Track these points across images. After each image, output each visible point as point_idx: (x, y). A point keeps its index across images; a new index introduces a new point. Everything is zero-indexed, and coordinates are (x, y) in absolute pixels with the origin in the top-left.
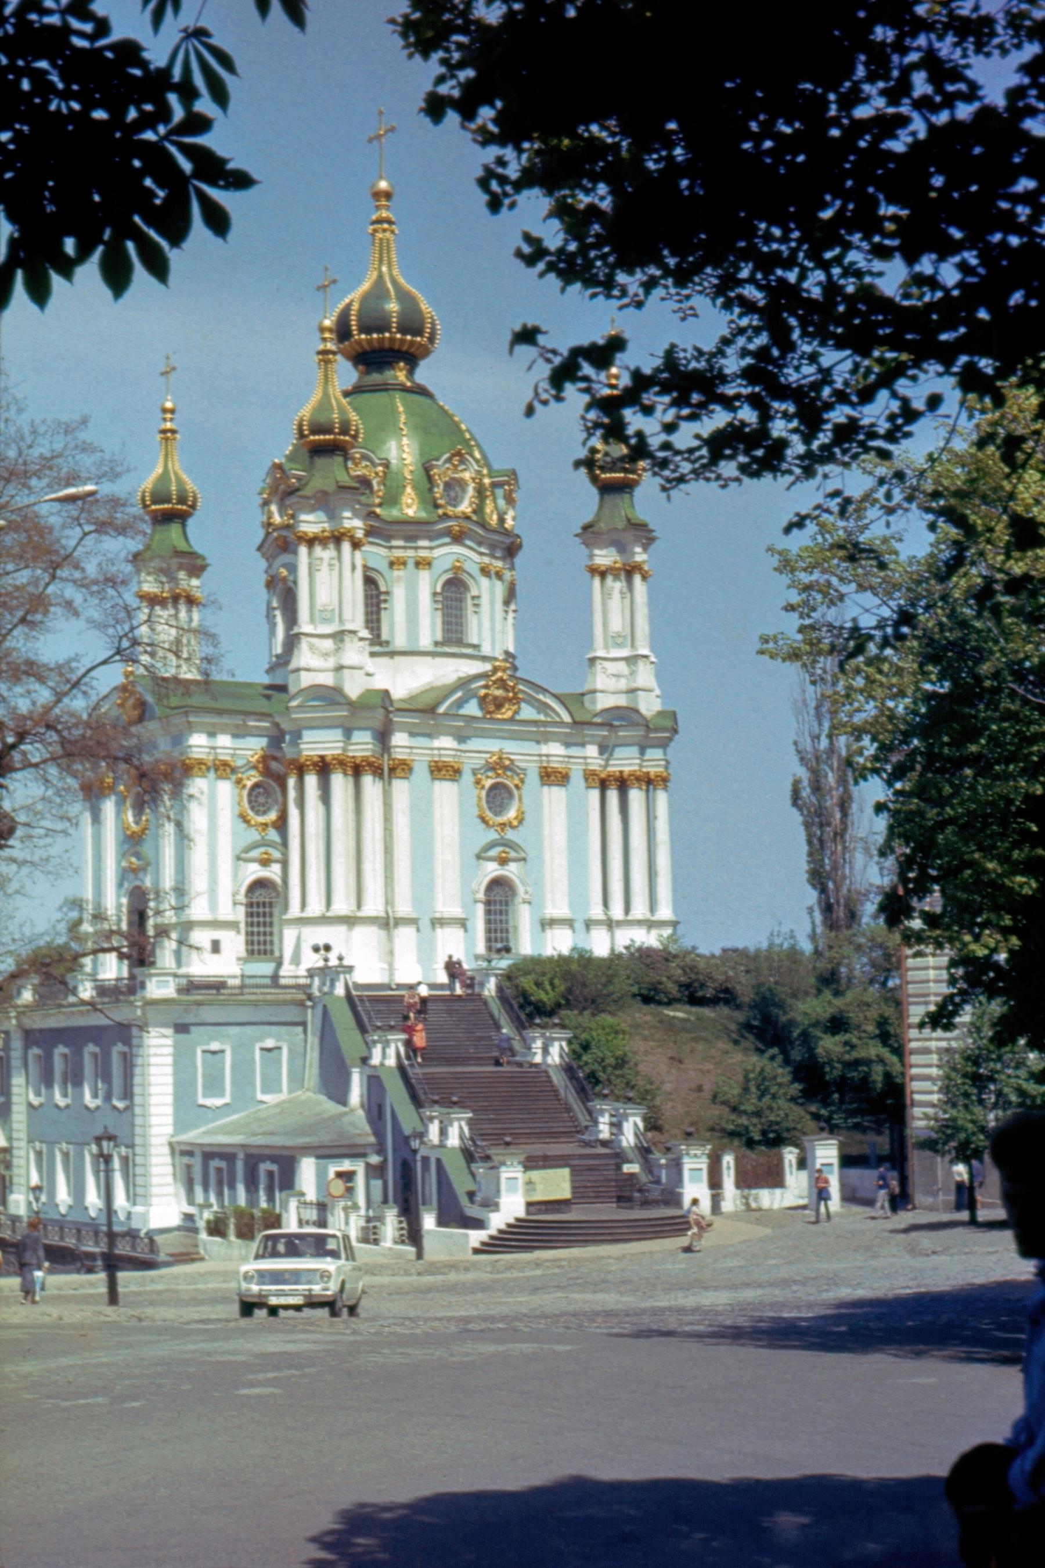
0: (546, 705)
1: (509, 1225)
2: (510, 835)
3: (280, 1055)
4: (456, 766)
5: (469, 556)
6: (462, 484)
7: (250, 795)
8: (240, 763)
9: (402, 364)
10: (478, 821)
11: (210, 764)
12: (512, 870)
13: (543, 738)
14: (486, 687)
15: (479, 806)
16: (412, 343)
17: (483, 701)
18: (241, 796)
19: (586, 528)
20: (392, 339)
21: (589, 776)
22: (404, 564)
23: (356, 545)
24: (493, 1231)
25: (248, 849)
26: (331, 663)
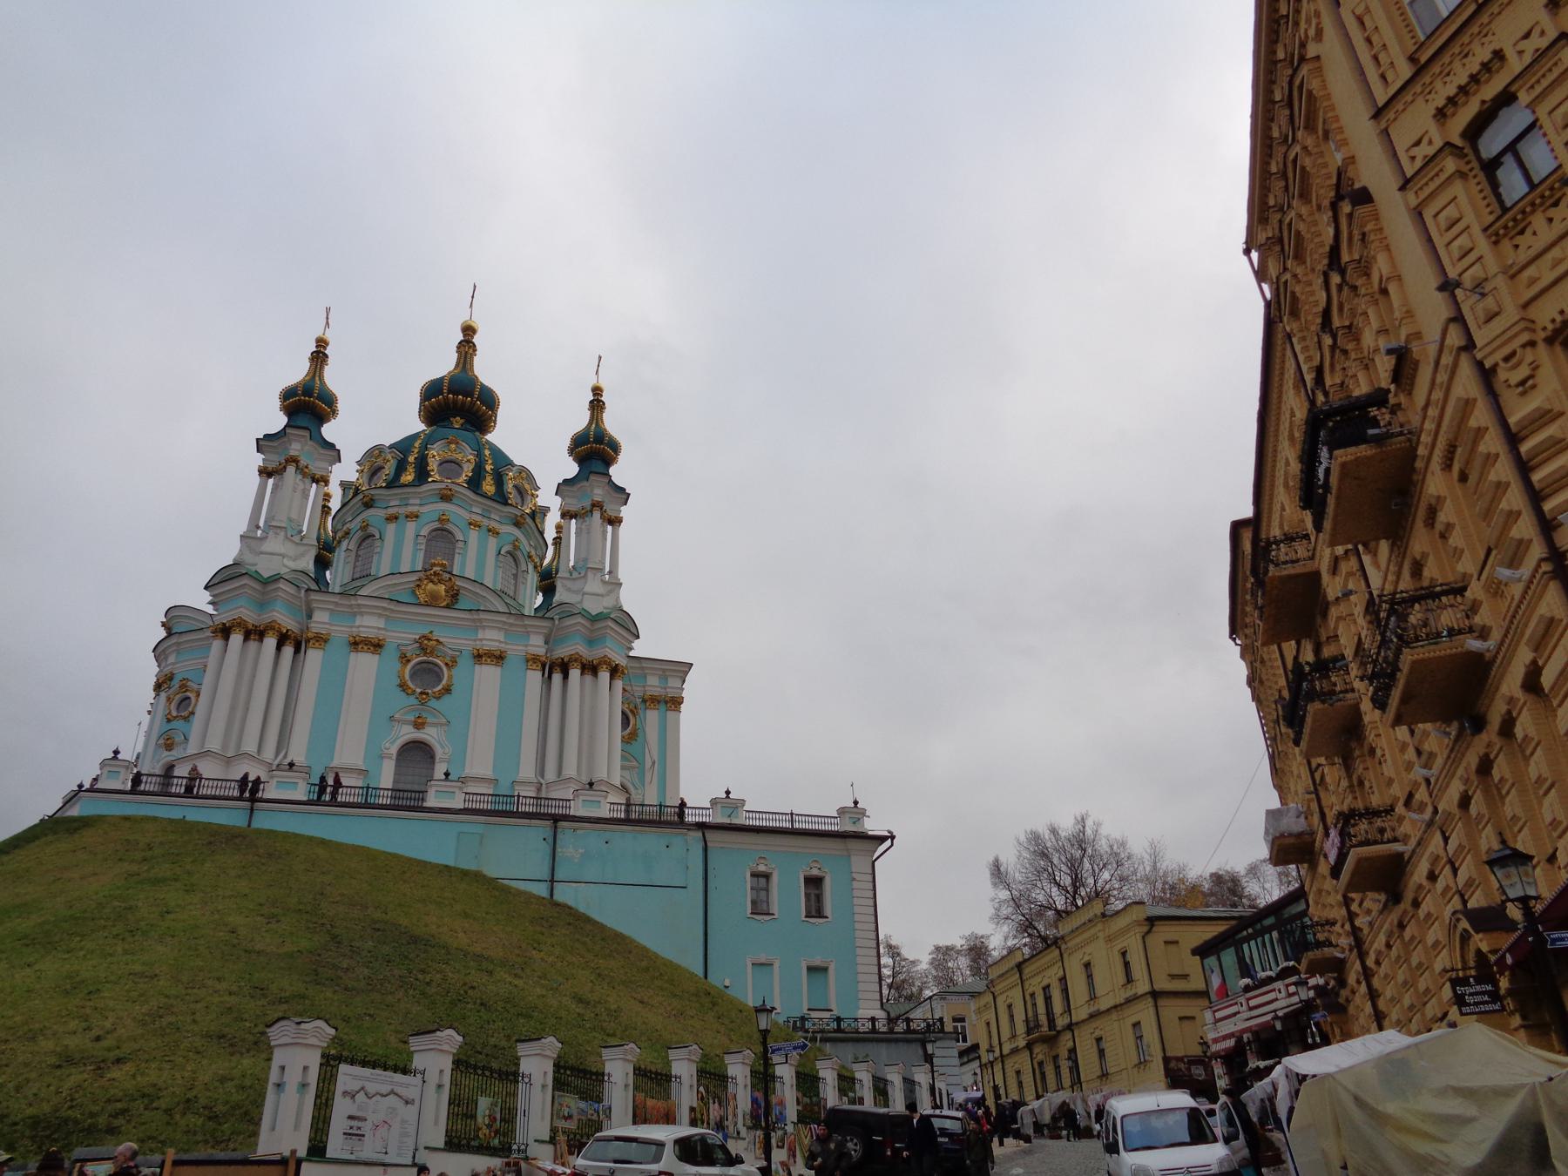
12: (430, 735)
13: (478, 626)
15: (401, 677)
21: (532, 660)
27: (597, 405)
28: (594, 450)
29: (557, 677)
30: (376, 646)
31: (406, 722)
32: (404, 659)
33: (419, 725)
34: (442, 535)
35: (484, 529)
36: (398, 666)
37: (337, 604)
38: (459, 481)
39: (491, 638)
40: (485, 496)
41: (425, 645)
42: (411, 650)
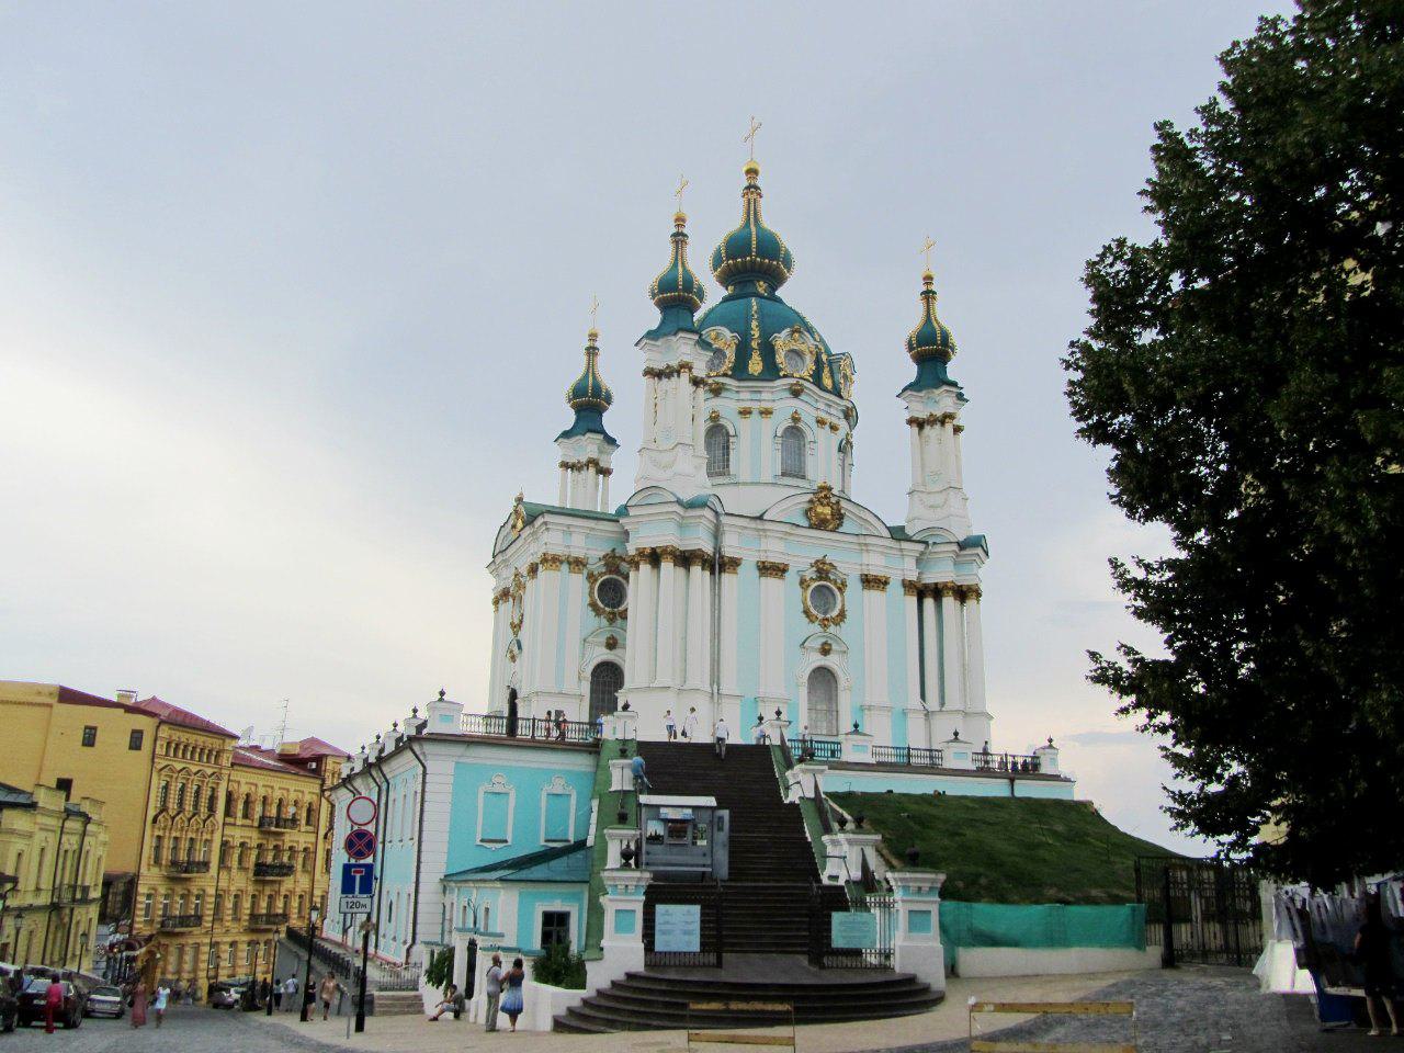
1: (614, 984)
2: (832, 629)
3: (569, 800)
4: (781, 567)
5: (810, 408)
6: (798, 354)
7: (600, 589)
8: (590, 561)
9: (761, 283)
12: (831, 661)
14: (811, 501)
15: (804, 603)
17: (807, 513)
18: (592, 589)
19: (905, 390)
20: (753, 262)
21: (909, 586)
22: (750, 413)
23: (696, 382)
24: (588, 992)
27: (928, 295)
28: (931, 353)
29: (929, 603)
30: (778, 570)
32: (802, 582)
33: (825, 650)
34: (794, 432)
35: (827, 427)
36: (799, 590)
37: (746, 528)
38: (805, 374)
39: (876, 564)
40: (825, 390)
41: (823, 570)
42: (810, 573)
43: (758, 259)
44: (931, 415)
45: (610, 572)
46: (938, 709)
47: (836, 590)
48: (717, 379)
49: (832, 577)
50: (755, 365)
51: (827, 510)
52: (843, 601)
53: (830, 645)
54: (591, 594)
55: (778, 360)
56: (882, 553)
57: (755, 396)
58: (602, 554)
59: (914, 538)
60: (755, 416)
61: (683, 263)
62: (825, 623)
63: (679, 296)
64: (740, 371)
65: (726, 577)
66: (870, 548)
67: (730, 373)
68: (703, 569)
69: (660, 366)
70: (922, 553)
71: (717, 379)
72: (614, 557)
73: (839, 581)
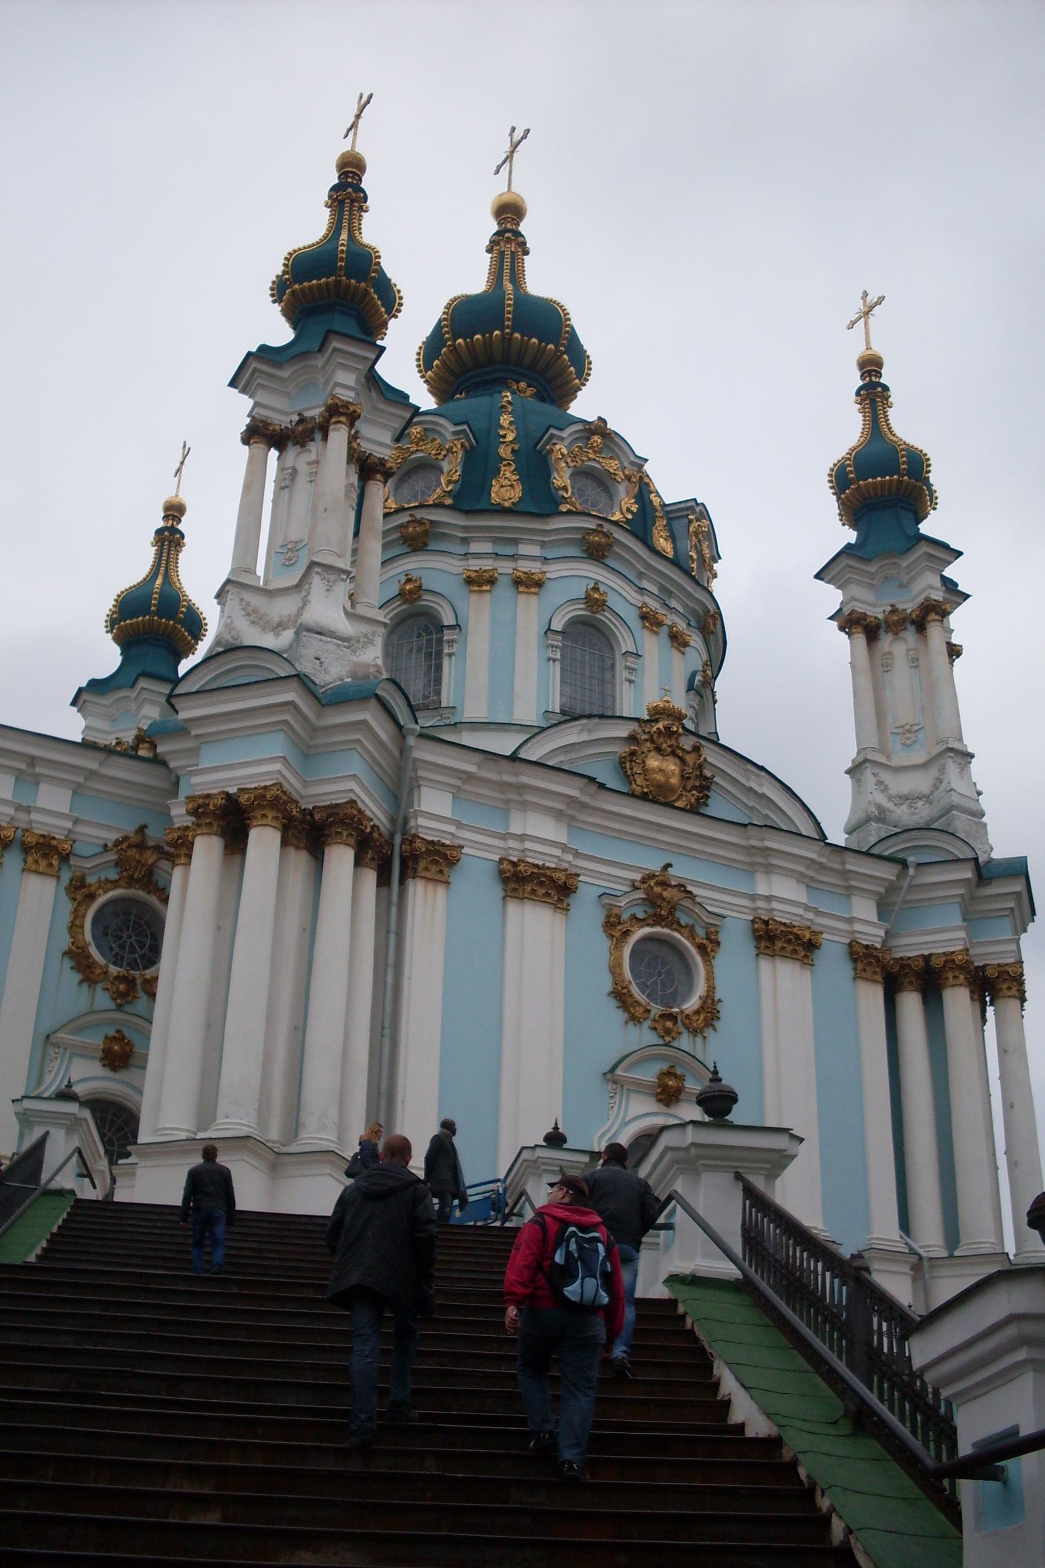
0: (763, 796)
2: (685, 1042)
4: (561, 877)
6: (602, 481)
8: (79, 849)
9: (523, 385)
10: (613, 1003)
11: (10, 833)
14: (632, 738)
15: (615, 969)
16: (540, 352)
17: (627, 764)
18: (77, 916)
20: (507, 340)
22: (492, 581)
23: (367, 468)
25: (77, 1024)
26: (288, 635)
27: (873, 395)
31: (639, 1087)
32: (614, 926)
37: (469, 777)
39: (786, 895)
41: (662, 898)
42: (629, 904)
43: (517, 335)
44: (894, 611)
45: (131, 882)
46: (944, 1253)
47: (693, 950)
48: (420, 514)
49: (684, 920)
50: (506, 488)
51: (672, 766)
52: (710, 977)
53: (681, 1078)
54: (75, 927)
55: (558, 482)
56: (802, 878)
57: (509, 550)
58: (113, 836)
59: (875, 851)
60: (503, 588)
61: (351, 236)
62: (669, 1024)
63: (338, 283)
64: (471, 497)
65: (418, 892)
66: (774, 861)
67: (449, 501)
68: (358, 862)
69: (283, 420)
70: (892, 888)
71: (420, 514)
72: (141, 846)
73: (700, 932)
